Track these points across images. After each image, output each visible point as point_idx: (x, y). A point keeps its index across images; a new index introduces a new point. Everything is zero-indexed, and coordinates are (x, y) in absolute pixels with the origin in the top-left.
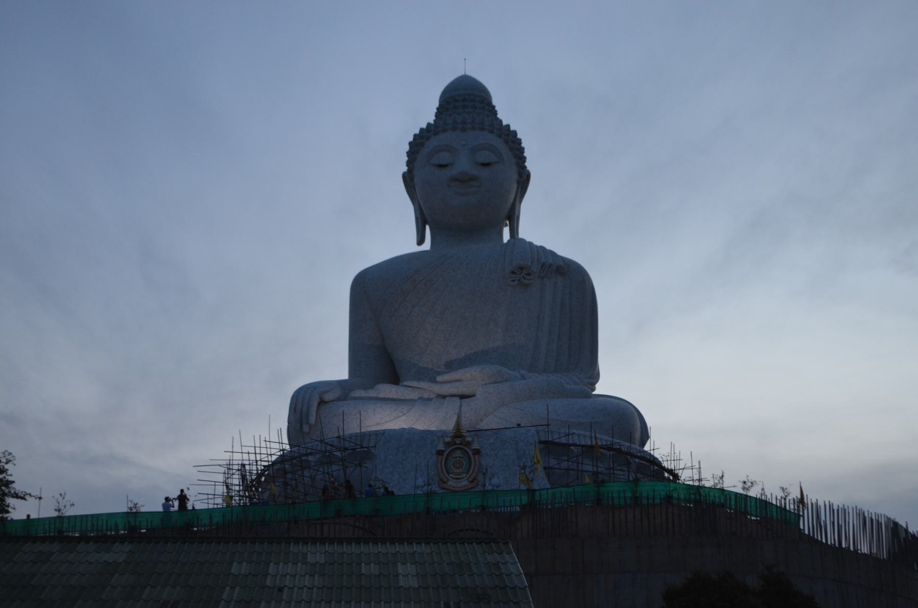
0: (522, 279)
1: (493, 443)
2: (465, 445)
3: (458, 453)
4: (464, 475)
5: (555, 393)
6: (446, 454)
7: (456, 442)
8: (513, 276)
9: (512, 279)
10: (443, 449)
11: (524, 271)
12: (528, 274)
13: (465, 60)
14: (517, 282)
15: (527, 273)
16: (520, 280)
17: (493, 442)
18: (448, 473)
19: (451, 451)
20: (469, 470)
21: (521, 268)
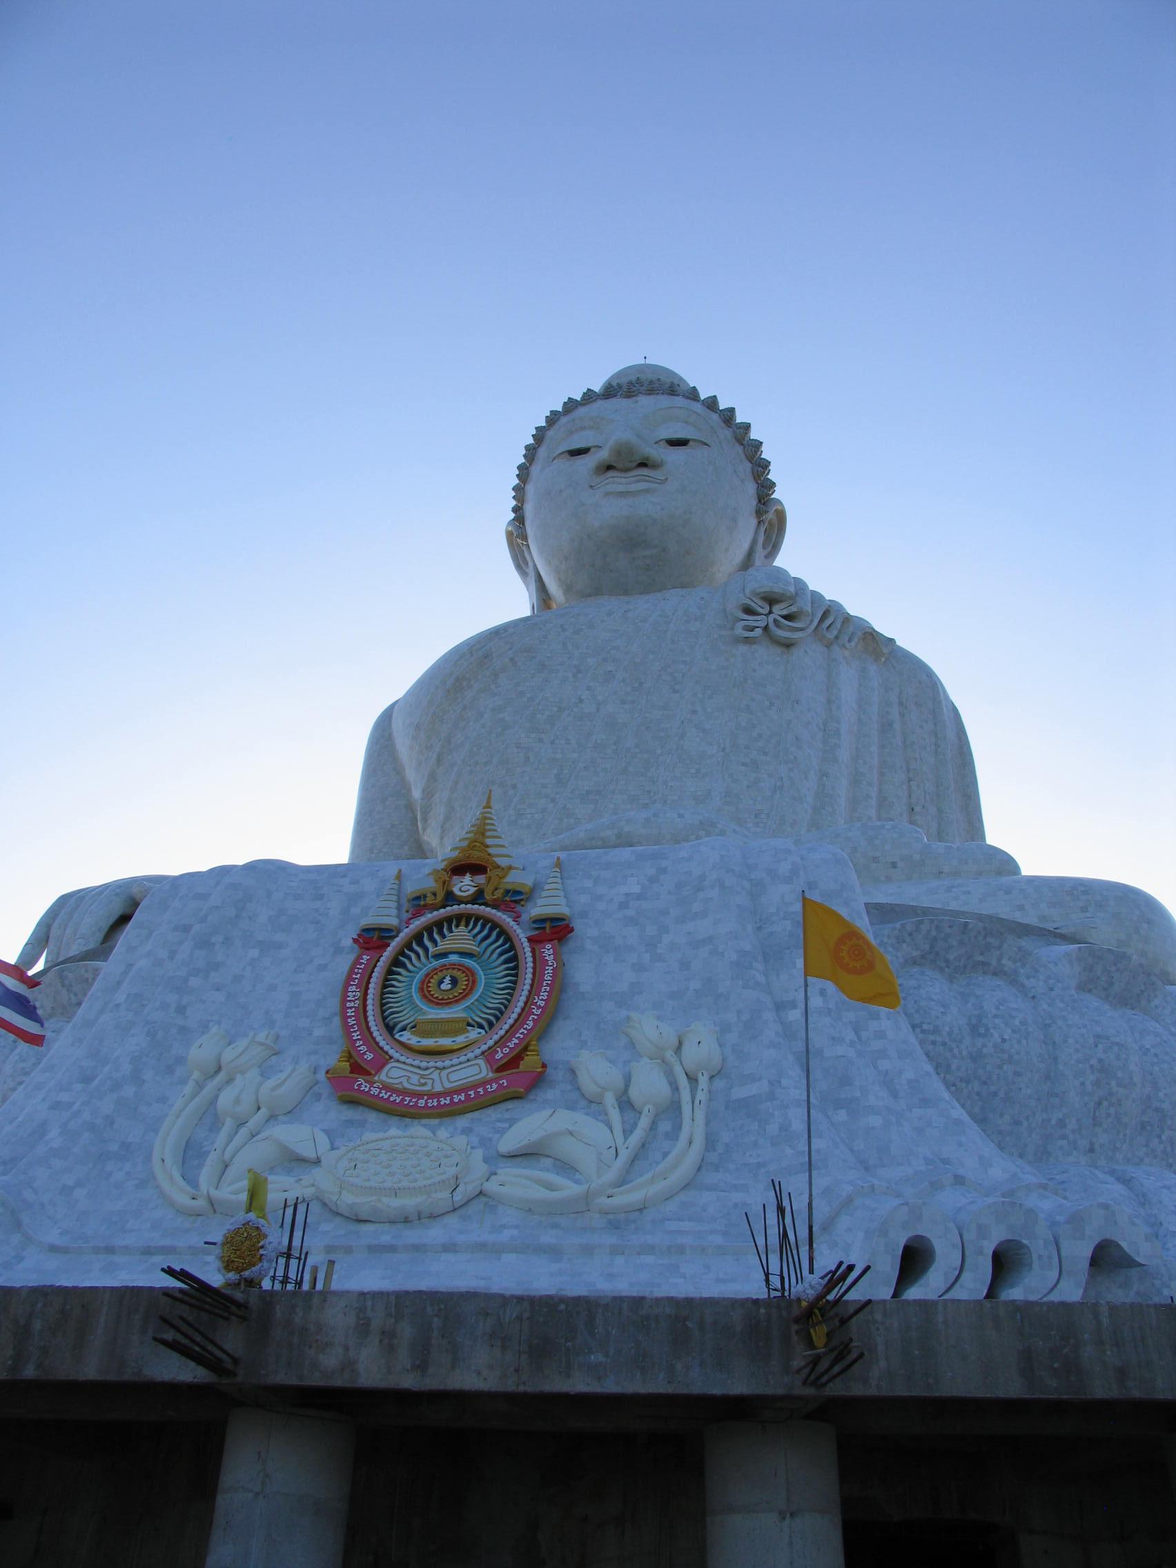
0: (771, 625)
1: (640, 897)
2: (495, 905)
3: (461, 938)
4: (474, 1034)
5: (894, 865)
6: (394, 944)
7: (456, 890)
8: (746, 617)
9: (746, 623)
10: (393, 921)
11: (779, 610)
12: (788, 617)
13: (645, 358)
14: (758, 632)
15: (785, 612)
16: (766, 628)
17: (637, 889)
18: (390, 1029)
19: (429, 929)
20: (500, 1014)
21: (771, 600)
